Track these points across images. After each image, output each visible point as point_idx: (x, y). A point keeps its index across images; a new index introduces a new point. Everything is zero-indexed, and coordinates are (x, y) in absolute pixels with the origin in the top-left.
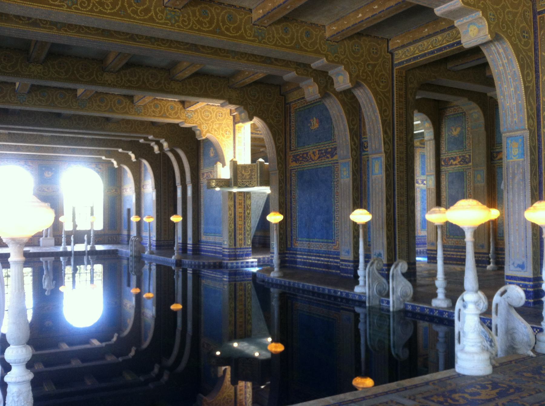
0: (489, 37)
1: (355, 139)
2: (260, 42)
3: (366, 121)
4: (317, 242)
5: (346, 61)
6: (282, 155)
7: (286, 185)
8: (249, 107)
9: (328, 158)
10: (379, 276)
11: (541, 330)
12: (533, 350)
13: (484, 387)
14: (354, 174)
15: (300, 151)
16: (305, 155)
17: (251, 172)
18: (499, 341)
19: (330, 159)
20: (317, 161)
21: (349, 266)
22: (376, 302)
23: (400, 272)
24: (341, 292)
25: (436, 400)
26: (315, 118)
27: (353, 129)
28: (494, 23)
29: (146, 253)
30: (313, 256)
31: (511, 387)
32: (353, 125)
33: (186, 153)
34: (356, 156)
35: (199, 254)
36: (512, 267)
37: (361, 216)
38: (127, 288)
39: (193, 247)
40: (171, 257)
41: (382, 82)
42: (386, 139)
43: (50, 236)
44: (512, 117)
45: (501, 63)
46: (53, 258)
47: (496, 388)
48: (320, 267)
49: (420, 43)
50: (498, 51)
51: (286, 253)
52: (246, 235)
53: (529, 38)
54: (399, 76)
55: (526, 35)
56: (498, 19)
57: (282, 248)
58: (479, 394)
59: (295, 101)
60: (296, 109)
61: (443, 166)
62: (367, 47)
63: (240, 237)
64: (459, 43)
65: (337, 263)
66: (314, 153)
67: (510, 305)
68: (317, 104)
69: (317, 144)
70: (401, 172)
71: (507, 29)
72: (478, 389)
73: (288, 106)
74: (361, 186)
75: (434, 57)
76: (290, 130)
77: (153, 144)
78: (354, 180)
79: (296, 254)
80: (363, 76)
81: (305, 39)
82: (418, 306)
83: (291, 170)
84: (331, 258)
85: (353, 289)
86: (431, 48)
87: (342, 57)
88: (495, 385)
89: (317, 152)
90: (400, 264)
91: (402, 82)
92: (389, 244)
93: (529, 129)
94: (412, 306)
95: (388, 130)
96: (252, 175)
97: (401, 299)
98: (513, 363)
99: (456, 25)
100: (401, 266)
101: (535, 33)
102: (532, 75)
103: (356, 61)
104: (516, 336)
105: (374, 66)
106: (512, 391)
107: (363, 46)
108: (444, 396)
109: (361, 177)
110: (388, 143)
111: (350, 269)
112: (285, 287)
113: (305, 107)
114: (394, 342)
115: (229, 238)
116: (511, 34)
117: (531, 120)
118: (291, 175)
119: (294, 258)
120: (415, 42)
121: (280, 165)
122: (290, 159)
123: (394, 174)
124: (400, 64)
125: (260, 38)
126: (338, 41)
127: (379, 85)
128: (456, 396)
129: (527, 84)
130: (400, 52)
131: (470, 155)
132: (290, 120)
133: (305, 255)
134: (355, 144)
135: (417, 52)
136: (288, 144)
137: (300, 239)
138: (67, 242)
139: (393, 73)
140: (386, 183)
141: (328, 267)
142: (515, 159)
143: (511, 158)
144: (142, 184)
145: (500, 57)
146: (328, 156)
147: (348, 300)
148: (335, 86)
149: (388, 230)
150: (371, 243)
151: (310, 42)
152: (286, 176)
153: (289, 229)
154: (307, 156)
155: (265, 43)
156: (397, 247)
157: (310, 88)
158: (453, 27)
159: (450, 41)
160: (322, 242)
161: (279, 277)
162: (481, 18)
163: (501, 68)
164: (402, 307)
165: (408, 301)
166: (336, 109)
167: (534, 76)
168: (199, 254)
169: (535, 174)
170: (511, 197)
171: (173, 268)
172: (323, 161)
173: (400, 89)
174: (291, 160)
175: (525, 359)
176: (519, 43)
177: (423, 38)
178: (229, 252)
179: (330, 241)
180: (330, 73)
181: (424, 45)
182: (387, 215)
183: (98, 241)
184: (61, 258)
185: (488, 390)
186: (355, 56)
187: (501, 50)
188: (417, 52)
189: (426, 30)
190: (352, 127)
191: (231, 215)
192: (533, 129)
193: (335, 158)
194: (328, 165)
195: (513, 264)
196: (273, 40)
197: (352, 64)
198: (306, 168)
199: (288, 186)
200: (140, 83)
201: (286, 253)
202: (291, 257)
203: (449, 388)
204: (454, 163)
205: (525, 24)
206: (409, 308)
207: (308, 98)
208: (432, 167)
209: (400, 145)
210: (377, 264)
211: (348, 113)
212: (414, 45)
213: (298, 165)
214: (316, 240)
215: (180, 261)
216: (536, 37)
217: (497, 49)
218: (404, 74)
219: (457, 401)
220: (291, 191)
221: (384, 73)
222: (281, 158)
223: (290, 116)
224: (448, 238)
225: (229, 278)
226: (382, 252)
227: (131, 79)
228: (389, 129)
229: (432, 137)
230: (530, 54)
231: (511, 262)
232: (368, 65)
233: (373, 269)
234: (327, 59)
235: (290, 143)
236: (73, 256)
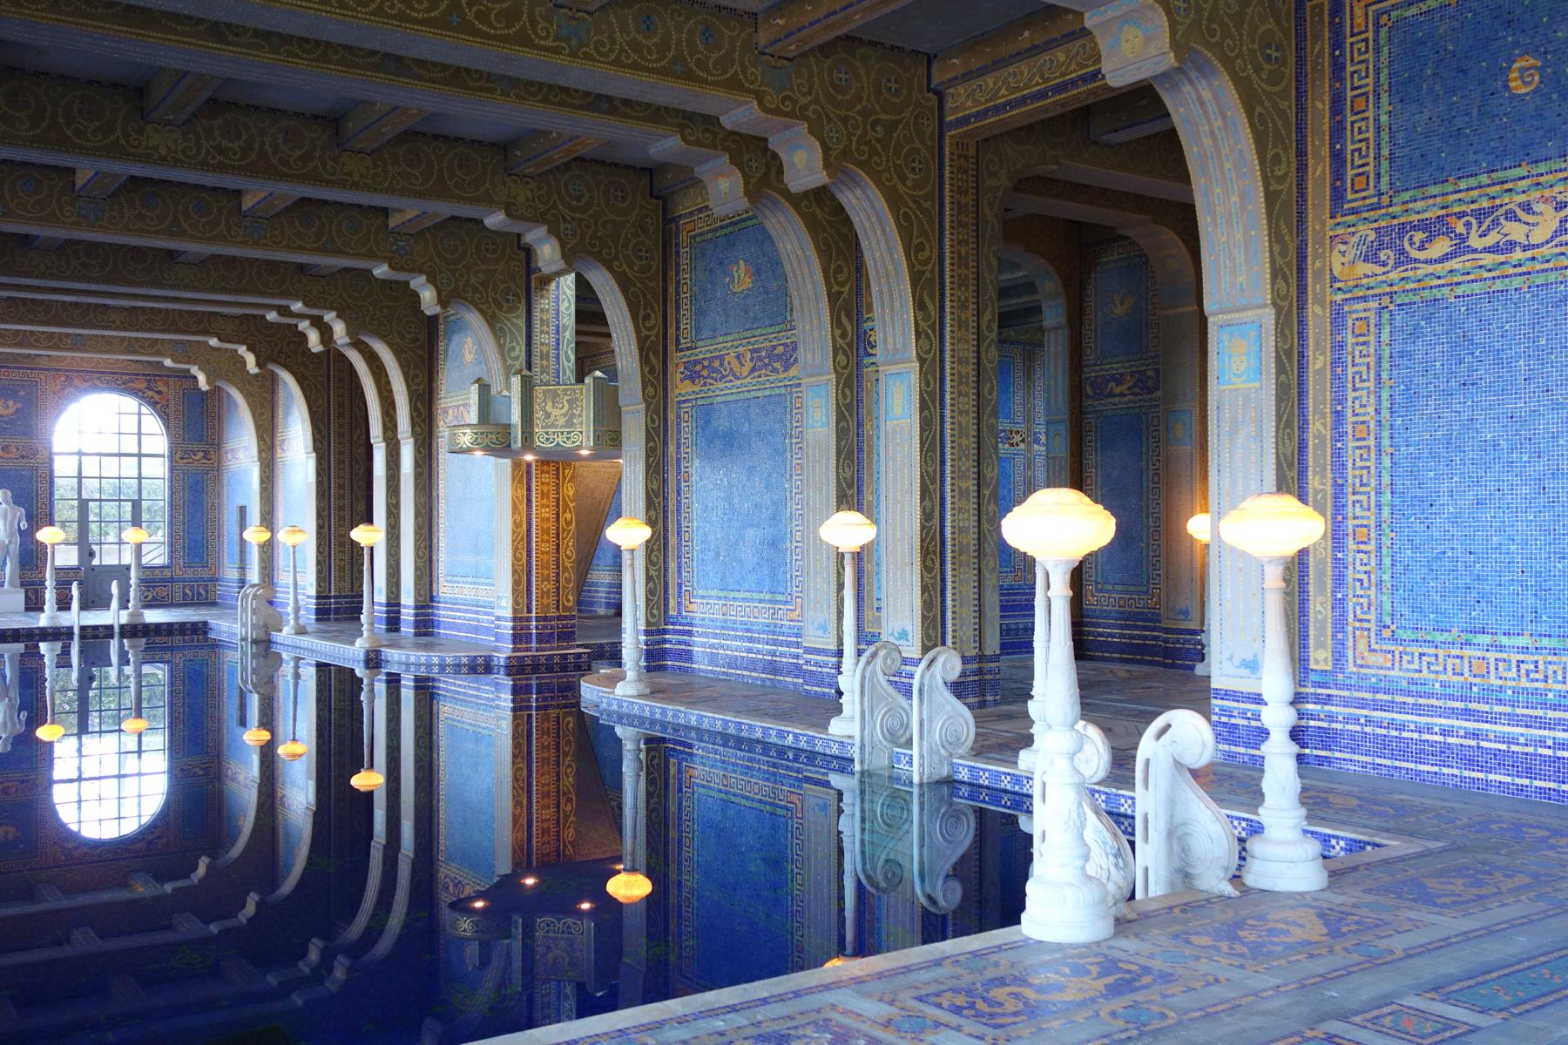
0: (1171, 60)
1: (844, 320)
2: (573, 54)
3: (872, 273)
5: (815, 111)
6: (654, 361)
7: (665, 443)
8: (562, 227)
10: (891, 690)
11: (1256, 829)
12: (1236, 879)
13: (1080, 971)
14: (840, 417)
15: (704, 351)
16: (717, 363)
17: (571, 408)
18: (1151, 854)
19: (782, 376)
21: (826, 665)
22: (880, 762)
23: (940, 682)
24: (796, 736)
25: (945, 1004)
27: (840, 293)
28: (1187, 21)
29: (286, 630)
30: (736, 638)
31: (1147, 970)
32: (839, 284)
33: (398, 353)
34: (845, 367)
35: (431, 634)
36: (1227, 667)
37: (847, 531)
38: (240, 729)
39: (416, 615)
40: (353, 643)
41: (914, 169)
42: (923, 325)
43: (12, 584)
44: (1234, 273)
45: (1206, 127)
46: (20, 647)
47: (1110, 974)
48: (755, 670)
49: (1011, 69)
50: (1199, 97)
51: (665, 632)
52: (562, 581)
53: (1282, 62)
54: (960, 156)
55: (1274, 54)
56: (1199, 10)
57: (653, 616)
58: (1061, 988)
59: (691, 214)
60: (694, 237)
61: (1088, 397)
62: (873, 75)
63: (546, 586)
64: (1096, 75)
65: (797, 657)
66: (738, 357)
67: (1178, 764)
68: (749, 223)
69: (747, 334)
70: (961, 412)
71: (1223, 39)
72: (1065, 975)
73: (673, 226)
74: (860, 450)
75: (1045, 109)
76: (678, 294)
77: (304, 325)
78: (841, 434)
79: (690, 633)
80: (862, 153)
81: (701, 48)
82: (984, 770)
84: (782, 644)
85: (824, 726)
86: (1038, 84)
87: (804, 101)
88: (1109, 966)
89: (749, 356)
90: (941, 659)
91: (965, 171)
92: (927, 605)
93: (1274, 304)
94: (971, 769)
95: (927, 300)
96: (573, 416)
97: (943, 752)
98: (1176, 911)
99: (1087, 24)
100: (944, 664)
101: (1300, 49)
102: (1289, 163)
103: (843, 113)
104: (1192, 842)
105: (891, 127)
106: (1147, 980)
107: (862, 72)
108: (969, 992)
109: (859, 424)
110: (927, 335)
113: (716, 230)
114: (921, 863)
115: (514, 591)
116: (1232, 50)
117: (1280, 281)
118: (679, 416)
119: (685, 643)
120: (997, 64)
121: (650, 390)
122: (676, 374)
123: (942, 417)
124: (960, 122)
125: (574, 42)
126: (791, 55)
127: (903, 179)
128: (999, 993)
129: (1274, 187)
130: (961, 90)
131: (1157, 371)
132: (678, 265)
133: (715, 636)
134: (844, 336)
135: (1003, 92)
136: (671, 331)
137: (701, 592)
138: (59, 602)
139: (941, 148)
140: (922, 443)
141: (773, 668)
142: (1239, 384)
143: (1230, 382)
144: (279, 437)
145: (1206, 112)
147: (812, 756)
148: (787, 177)
149: (926, 568)
150: (883, 604)
151: (715, 56)
152: (666, 420)
153: (672, 565)
155: (587, 57)
156: (949, 614)
158: (1085, 32)
159: (1087, 66)
160: (760, 601)
161: (640, 696)
162: (1150, 7)
163: (1208, 142)
164: (945, 772)
165: (961, 757)
166: (794, 243)
167: (1294, 166)
168: (431, 634)
169: (1289, 424)
170: (1226, 482)
171: (358, 673)
173: (962, 191)
174: (679, 376)
175: (1210, 901)
176: (1254, 76)
177: (1018, 54)
179: (780, 597)
180: (774, 143)
181: (1022, 73)
182: (923, 527)
183: (154, 599)
184: (43, 647)
185: (1086, 979)
186: (839, 97)
187: (1207, 95)
188: (1003, 92)
189: (1026, 34)
190: (835, 288)
191: (516, 525)
192: (1286, 304)
193: (792, 372)
194: (778, 391)
195: (1231, 659)
196: (612, 50)
197: (829, 120)
198: (719, 399)
199: (672, 448)
200: (253, 156)
201: (665, 632)
202: (679, 643)
203: (991, 973)
204: (1118, 390)
205: (1270, 25)
206: (964, 775)
207: (718, 211)
208: (1060, 398)
209: (959, 340)
210: (885, 658)
211: (824, 251)
212: (998, 73)
213: (697, 389)
214: (742, 595)
215: (378, 652)
216: (1301, 61)
217: (1196, 90)
218: (972, 151)
219: (1000, 1004)
220: (678, 460)
221: (918, 145)
222: (652, 371)
223: (678, 253)
224: (1101, 591)
225: (514, 701)
226: (909, 629)
227: (225, 143)
228: (932, 298)
229: (1063, 320)
230: (1283, 104)
231: (1226, 655)
232: (873, 125)
233: (874, 672)
234: (761, 104)
235: (678, 328)
236: (76, 638)
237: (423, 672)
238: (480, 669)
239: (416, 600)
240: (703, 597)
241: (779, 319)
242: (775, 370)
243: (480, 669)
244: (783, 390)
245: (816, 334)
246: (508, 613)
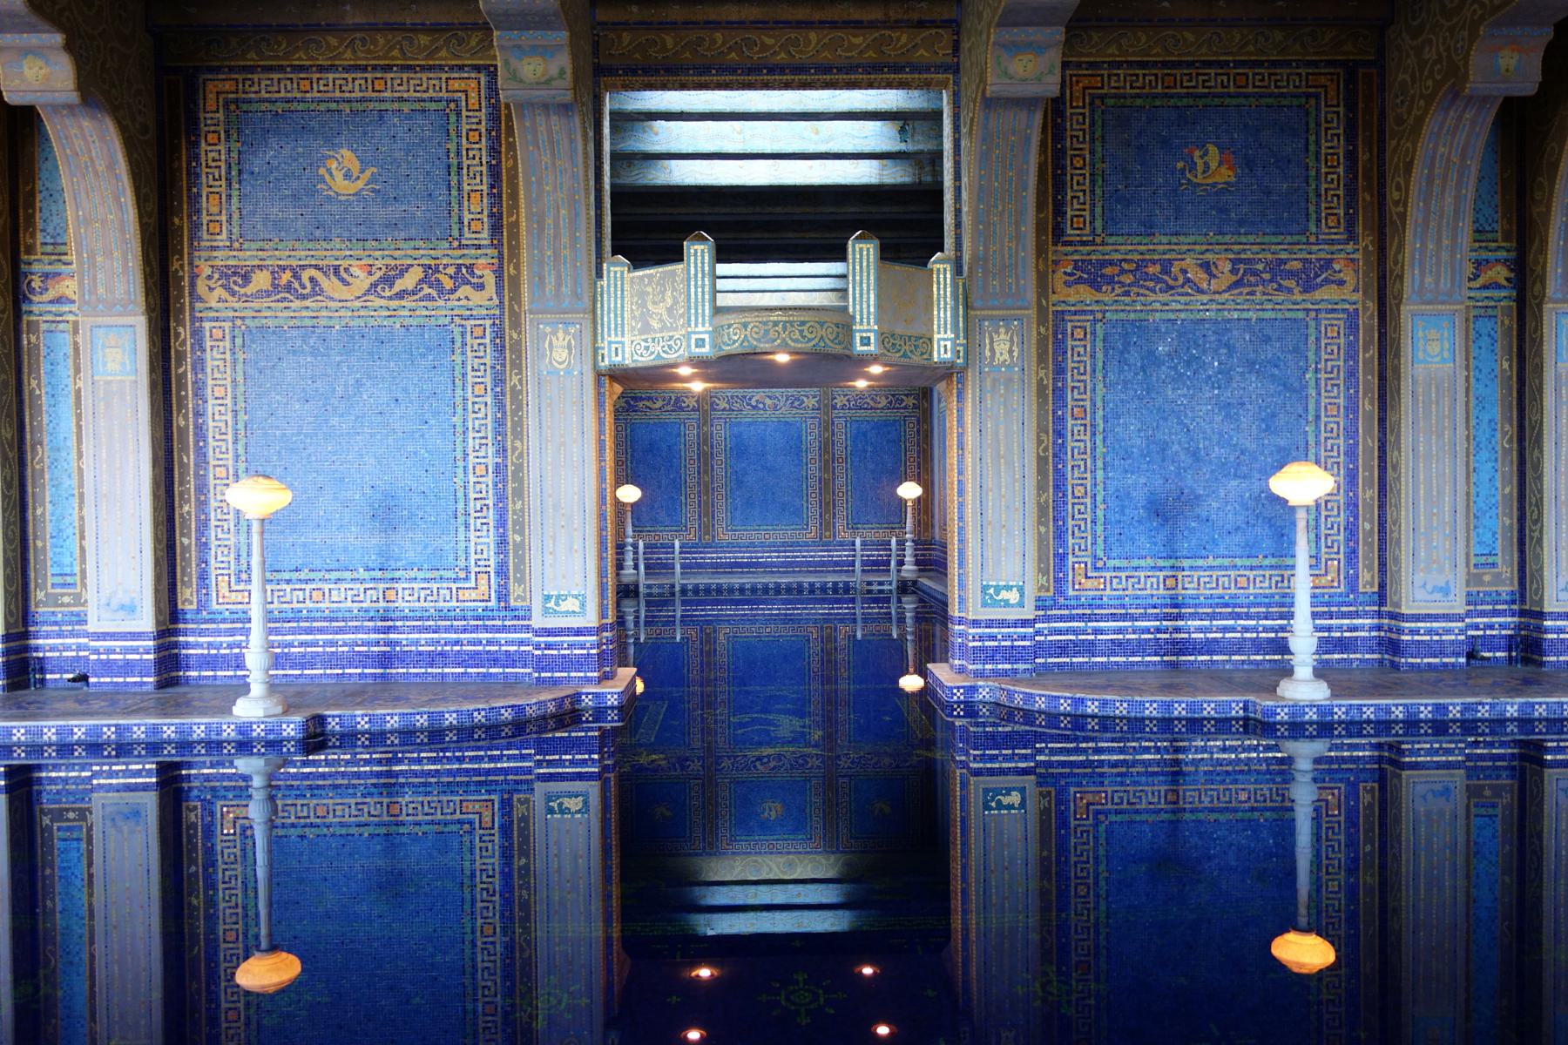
4: (1221, 568)
9: (1290, 291)
19: (1299, 298)
20: (1226, 295)
26: (1213, 150)
39: (158, 649)
48: (1238, 653)
59: (1092, 65)
60: (1102, 97)
66: (1206, 266)
69: (1227, 238)
83: (1063, 312)
89: (1228, 266)
111: (1452, 642)
112: (1354, 727)
113: (1155, 96)
137: (1111, 563)
146: (1291, 283)
154: (1166, 271)
157: (1506, 52)
160: (1252, 568)
172: (1258, 297)
178: (599, 645)
194: (1288, 315)
237: (20, 758)
238: (568, 720)
239: (158, 623)
240: (1115, 569)
241: (1295, 228)
242: (1280, 288)
243: (568, 720)
244: (1301, 315)
245: (1445, 256)
246: (591, 619)
